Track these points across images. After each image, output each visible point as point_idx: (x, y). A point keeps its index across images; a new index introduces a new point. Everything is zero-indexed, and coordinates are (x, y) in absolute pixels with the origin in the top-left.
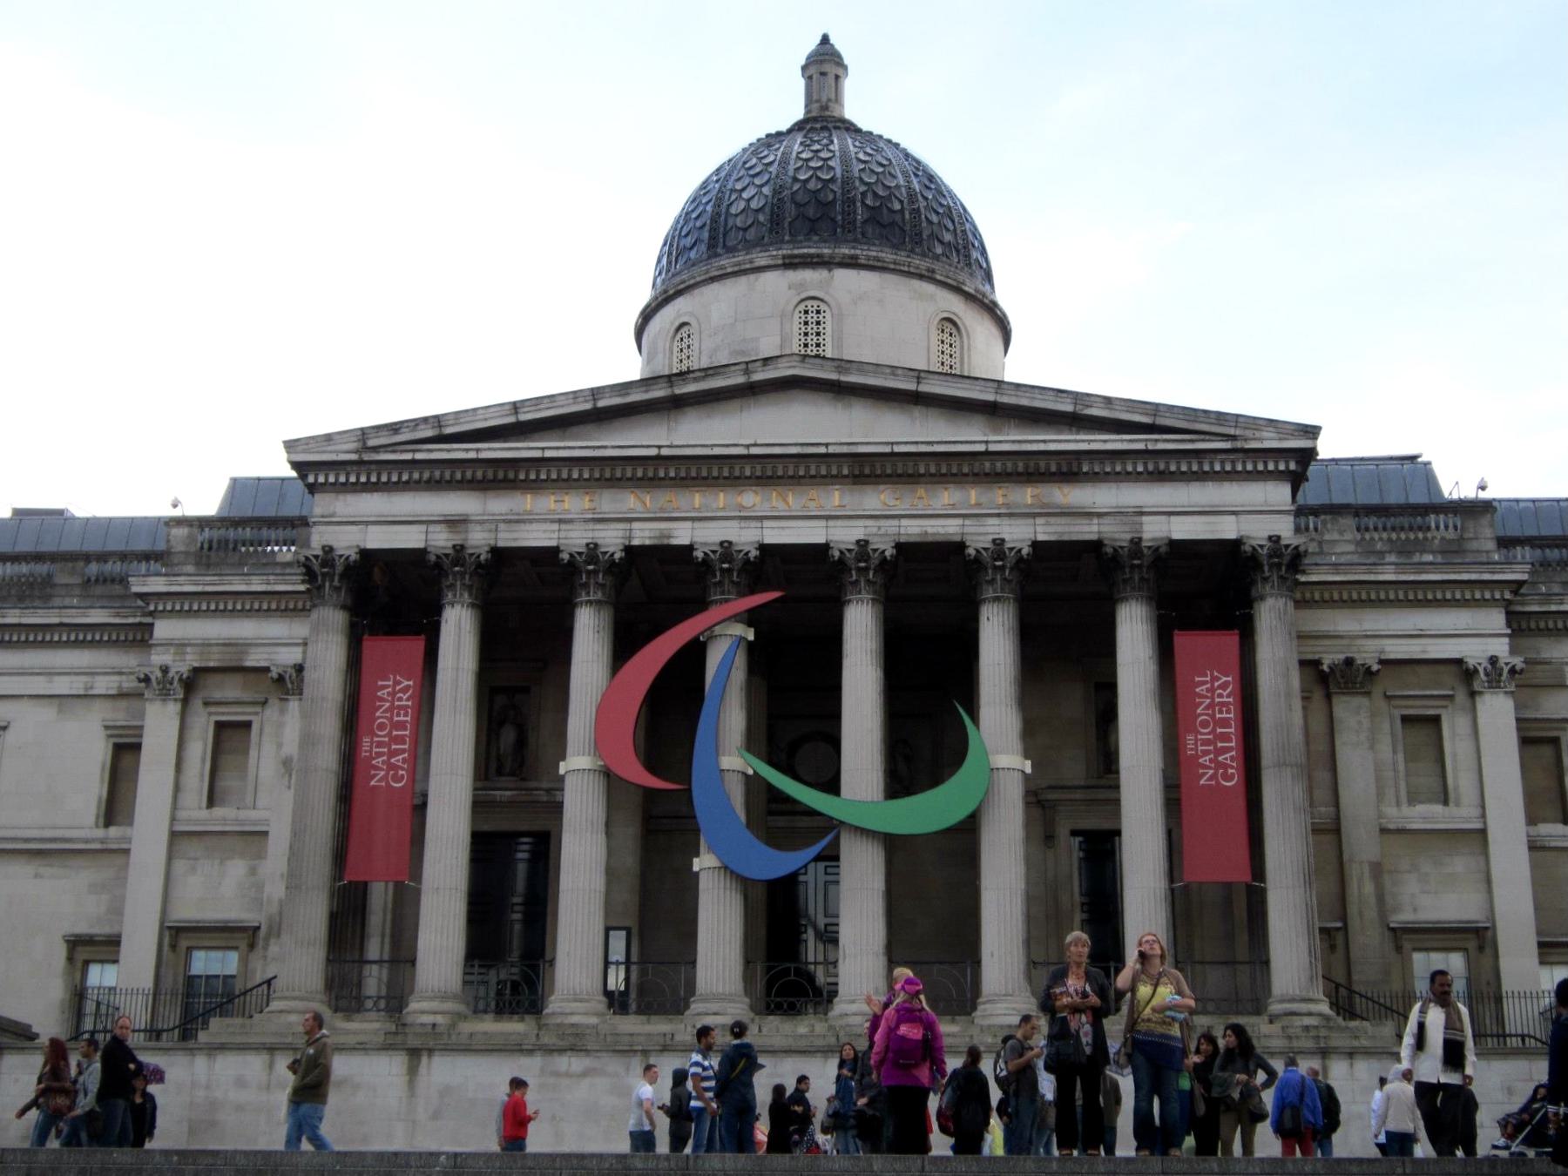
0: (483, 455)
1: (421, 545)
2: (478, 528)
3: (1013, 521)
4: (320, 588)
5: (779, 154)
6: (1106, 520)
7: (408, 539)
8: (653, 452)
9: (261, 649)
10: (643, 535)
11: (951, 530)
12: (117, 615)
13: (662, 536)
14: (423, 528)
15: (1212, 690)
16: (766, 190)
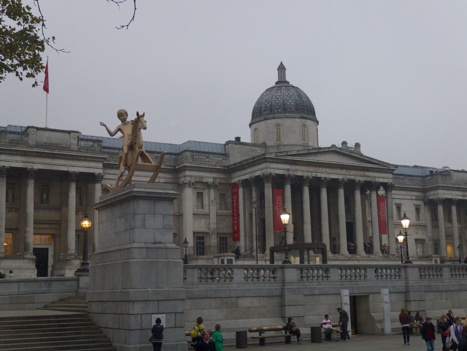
0: (294, 159)
1: (283, 174)
2: (291, 171)
3: (361, 177)
4: (269, 180)
5: (292, 92)
6: (372, 178)
7: (281, 172)
8: (317, 161)
9: (206, 178)
10: (314, 174)
11: (353, 178)
12: (166, 166)
13: (316, 175)
14: (283, 170)
15: (382, 205)
16: (293, 101)
